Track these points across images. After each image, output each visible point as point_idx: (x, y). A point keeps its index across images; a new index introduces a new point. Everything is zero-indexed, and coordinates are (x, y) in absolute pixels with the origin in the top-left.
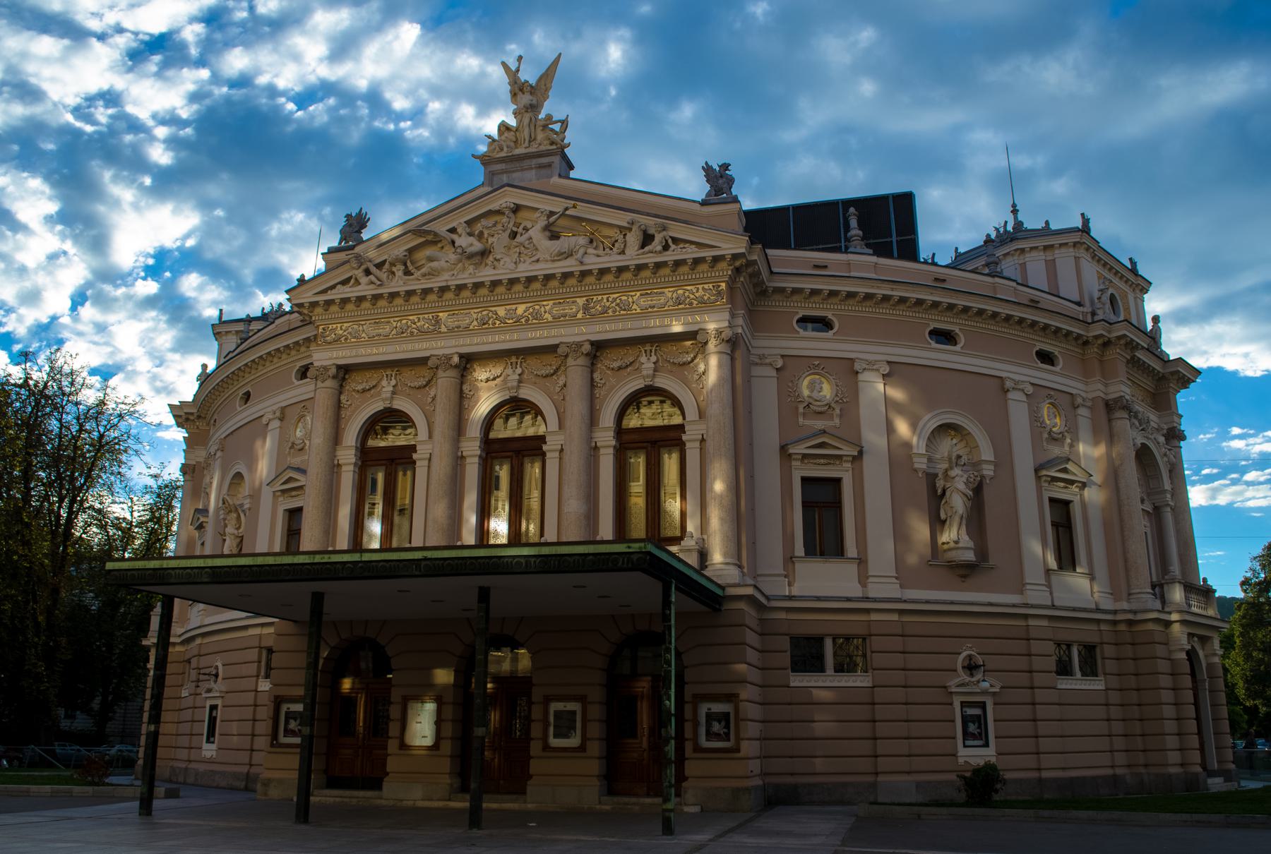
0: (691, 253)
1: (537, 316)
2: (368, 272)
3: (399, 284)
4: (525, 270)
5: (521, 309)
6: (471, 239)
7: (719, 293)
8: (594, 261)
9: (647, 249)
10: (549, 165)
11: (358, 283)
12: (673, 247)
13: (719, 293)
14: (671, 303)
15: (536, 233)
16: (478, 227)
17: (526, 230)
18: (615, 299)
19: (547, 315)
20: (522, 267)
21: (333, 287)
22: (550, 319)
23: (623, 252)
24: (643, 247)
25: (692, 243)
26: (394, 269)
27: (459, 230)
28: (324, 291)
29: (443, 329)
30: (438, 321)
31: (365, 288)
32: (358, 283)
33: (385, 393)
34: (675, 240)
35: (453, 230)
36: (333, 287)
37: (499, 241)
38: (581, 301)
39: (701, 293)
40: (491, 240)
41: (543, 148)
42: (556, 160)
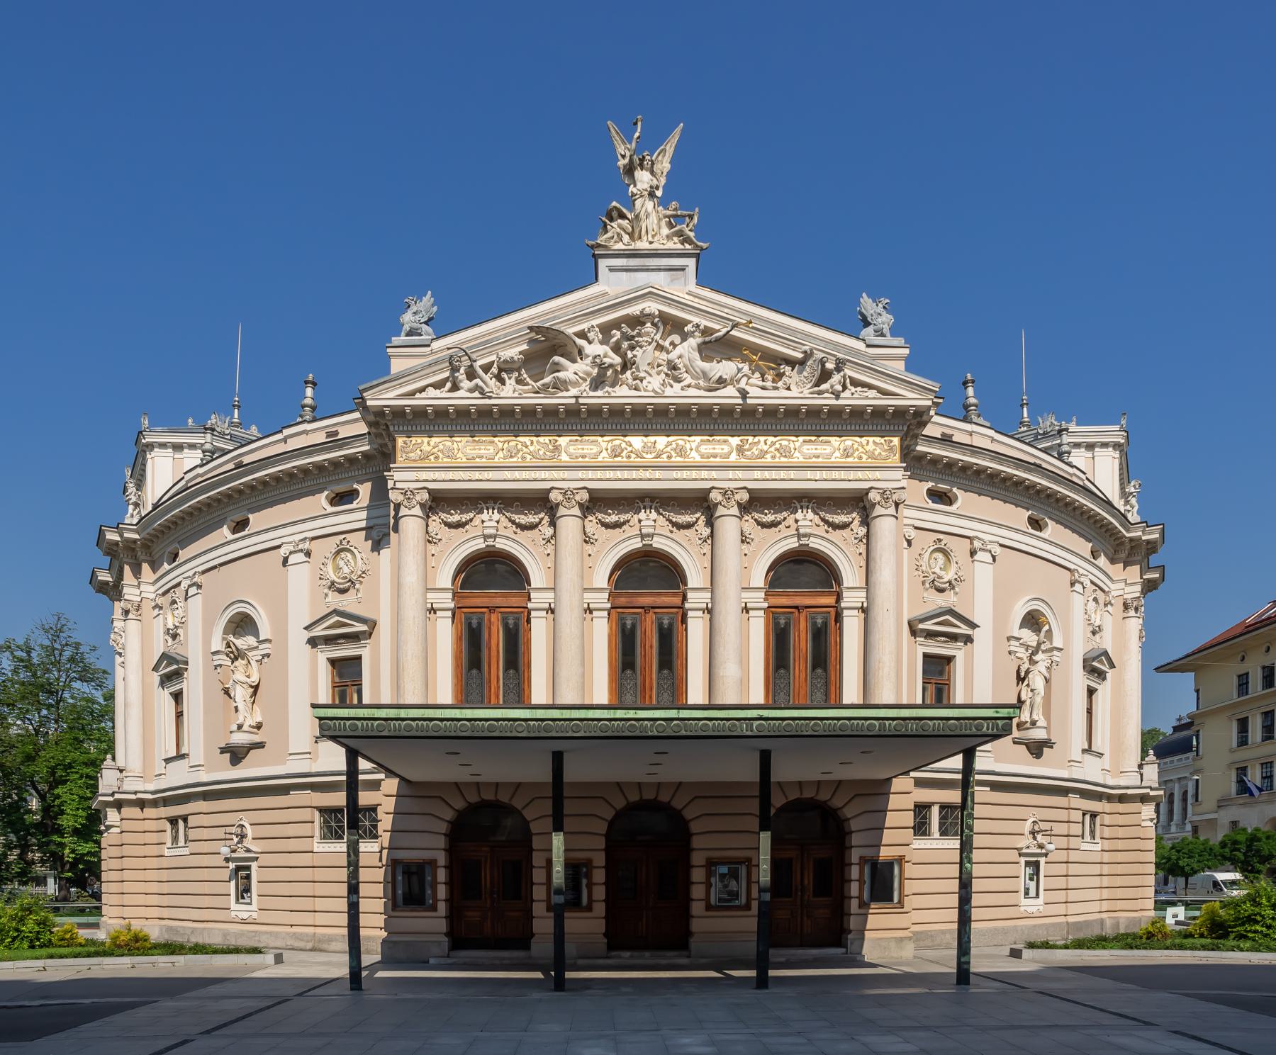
0: (870, 399)
1: (681, 451)
2: (471, 375)
3: (510, 393)
4: (676, 394)
5: (661, 441)
6: (606, 349)
7: (891, 449)
8: (761, 393)
9: (824, 387)
10: (682, 269)
11: (455, 387)
12: (853, 389)
13: (891, 449)
14: (837, 454)
15: (686, 350)
16: (617, 334)
17: (673, 345)
18: (774, 444)
19: (694, 454)
20: (669, 391)
21: (422, 390)
22: (698, 459)
23: (789, 389)
24: (817, 385)
25: (870, 387)
26: (504, 375)
27: (591, 335)
28: (411, 394)
29: (564, 457)
30: (557, 448)
31: (464, 397)
32: (455, 387)
33: (490, 529)
34: (855, 383)
35: (582, 335)
36: (422, 390)
37: (644, 356)
38: (735, 441)
39: (871, 447)
40: (630, 354)
41: (670, 245)
42: (691, 263)
